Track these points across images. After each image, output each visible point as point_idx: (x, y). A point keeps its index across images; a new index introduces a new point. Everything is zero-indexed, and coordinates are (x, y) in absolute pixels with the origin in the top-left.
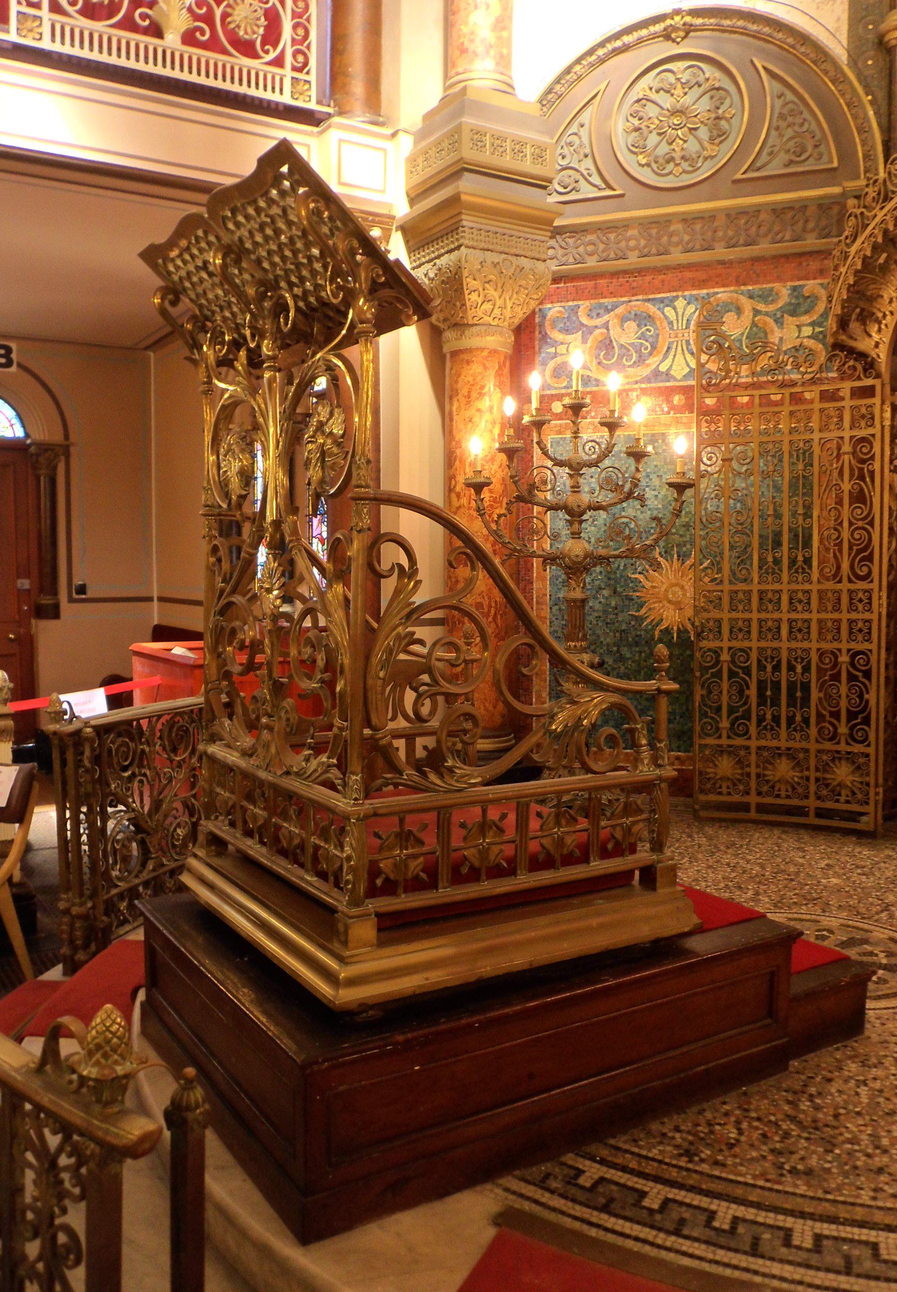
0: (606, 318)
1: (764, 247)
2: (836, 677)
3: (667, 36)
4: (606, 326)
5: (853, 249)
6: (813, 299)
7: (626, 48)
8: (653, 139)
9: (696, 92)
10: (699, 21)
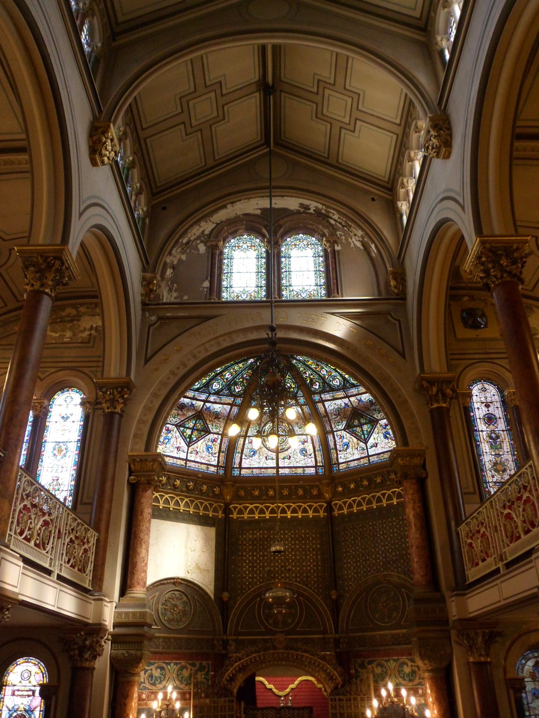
0: (152, 667)
3: (174, 583)
4: (151, 670)
5: (236, 664)
6: (205, 667)
7: (164, 584)
8: (168, 613)
9: (180, 601)
10: (182, 582)
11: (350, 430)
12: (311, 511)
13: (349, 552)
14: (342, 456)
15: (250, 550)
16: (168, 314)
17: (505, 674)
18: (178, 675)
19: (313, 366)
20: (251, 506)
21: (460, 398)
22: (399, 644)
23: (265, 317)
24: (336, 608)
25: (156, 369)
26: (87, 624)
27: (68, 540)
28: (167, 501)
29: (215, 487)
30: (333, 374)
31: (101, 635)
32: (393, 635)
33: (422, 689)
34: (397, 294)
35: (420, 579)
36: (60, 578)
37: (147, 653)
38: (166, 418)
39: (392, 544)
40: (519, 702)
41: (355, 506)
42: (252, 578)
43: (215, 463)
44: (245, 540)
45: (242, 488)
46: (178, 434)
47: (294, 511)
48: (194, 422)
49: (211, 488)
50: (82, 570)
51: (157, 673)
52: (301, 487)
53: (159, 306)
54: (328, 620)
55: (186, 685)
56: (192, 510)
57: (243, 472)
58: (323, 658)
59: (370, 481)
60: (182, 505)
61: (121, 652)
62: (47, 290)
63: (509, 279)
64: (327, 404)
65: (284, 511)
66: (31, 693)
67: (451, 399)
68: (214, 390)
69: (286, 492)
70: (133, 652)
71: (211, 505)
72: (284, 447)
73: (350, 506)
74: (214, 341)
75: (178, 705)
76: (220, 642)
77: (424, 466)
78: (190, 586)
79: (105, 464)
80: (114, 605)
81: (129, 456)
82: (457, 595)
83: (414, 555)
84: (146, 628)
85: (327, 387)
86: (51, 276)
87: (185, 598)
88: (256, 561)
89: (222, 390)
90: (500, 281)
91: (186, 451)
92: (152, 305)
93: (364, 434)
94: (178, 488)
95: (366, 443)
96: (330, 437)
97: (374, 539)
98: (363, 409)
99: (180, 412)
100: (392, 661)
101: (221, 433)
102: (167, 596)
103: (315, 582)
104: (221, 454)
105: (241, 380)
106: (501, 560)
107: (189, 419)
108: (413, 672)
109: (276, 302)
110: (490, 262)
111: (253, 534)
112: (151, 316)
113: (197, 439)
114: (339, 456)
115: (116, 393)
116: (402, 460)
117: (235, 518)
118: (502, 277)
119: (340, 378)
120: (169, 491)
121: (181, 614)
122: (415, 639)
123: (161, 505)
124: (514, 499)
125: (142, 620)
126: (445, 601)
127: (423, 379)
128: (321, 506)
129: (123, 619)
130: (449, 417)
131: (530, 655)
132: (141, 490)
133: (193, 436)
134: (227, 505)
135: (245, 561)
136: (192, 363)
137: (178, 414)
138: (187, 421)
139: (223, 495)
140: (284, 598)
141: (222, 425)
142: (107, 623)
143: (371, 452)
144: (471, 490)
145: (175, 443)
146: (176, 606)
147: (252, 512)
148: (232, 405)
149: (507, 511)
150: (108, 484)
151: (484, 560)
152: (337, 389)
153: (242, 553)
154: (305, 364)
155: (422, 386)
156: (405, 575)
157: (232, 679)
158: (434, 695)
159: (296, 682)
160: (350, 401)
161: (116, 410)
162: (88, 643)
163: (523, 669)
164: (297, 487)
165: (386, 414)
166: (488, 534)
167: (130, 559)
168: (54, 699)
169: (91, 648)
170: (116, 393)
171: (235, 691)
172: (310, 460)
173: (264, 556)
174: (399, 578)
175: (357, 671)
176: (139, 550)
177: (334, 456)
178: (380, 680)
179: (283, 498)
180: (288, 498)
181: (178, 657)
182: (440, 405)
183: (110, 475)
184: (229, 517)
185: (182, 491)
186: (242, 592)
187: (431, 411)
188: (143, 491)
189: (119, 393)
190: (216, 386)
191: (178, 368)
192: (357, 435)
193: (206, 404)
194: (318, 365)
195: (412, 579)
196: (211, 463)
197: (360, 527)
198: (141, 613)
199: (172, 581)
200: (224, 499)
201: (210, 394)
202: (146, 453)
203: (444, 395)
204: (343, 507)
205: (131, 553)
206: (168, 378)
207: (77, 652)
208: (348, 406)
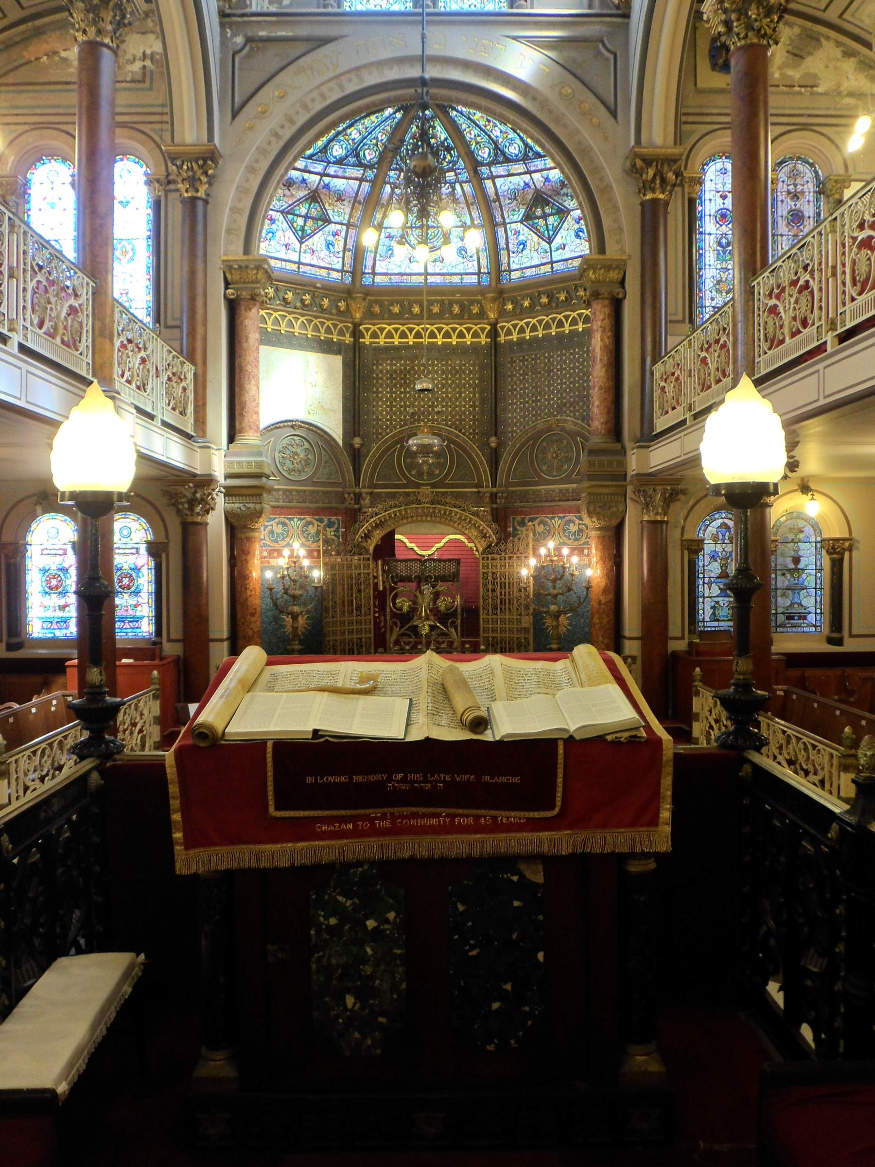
1: (321, 505)
2: (361, 646)
3: (292, 427)
6: (334, 523)
7: (280, 427)
8: (288, 462)
11: (530, 222)
12: (472, 335)
13: (516, 390)
14: (516, 260)
15: (388, 386)
16: (262, 33)
17: (682, 534)
18: (303, 532)
19: (482, 123)
20: (388, 328)
21: (686, 186)
22: (568, 500)
23: (408, 42)
24: (494, 459)
25: (251, 128)
26: (195, 475)
27: (166, 378)
28: (276, 322)
29: (340, 301)
30: (509, 137)
31: (212, 487)
32: (561, 491)
33: (588, 549)
34: (618, 7)
35: (599, 427)
36: (165, 424)
37: (267, 507)
38: (269, 203)
39: (571, 383)
40: (692, 565)
41: (528, 331)
42: (391, 420)
43: (339, 266)
44: (381, 372)
45: (376, 302)
46: (285, 225)
47: (447, 335)
48: (307, 206)
49: (334, 302)
50: (183, 413)
51: (279, 529)
52: (457, 302)
53: (246, 19)
54: (485, 472)
55: (314, 542)
56: (310, 333)
57: (378, 279)
58: (476, 514)
59: (551, 296)
60: (297, 325)
61: (236, 506)
62: (107, 41)
63: (755, 41)
64: (499, 182)
65: (432, 335)
66: (134, 551)
67: (674, 185)
68: (335, 157)
69: (436, 309)
70: (251, 505)
71: (335, 326)
72: (435, 244)
73: (522, 331)
74: (334, 82)
75: (306, 563)
76: (352, 495)
77: (622, 283)
78: (312, 430)
79: (192, 273)
80: (223, 453)
81: (223, 261)
82: (639, 447)
83: (595, 398)
84: (264, 480)
85: (500, 156)
86: (108, 16)
87: (307, 445)
88: (395, 399)
89: (347, 157)
90: (743, 42)
91: (298, 250)
92: (235, 15)
93: (548, 230)
94: (289, 303)
95: (550, 243)
96: (501, 231)
97: (549, 374)
98: (549, 193)
99: (287, 192)
100: (557, 519)
101: (345, 222)
102: (285, 442)
103: (470, 427)
104: (347, 253)
105: (374, 141)
106: (690, 410)
107: (300, 201)
108: (581, 531)
109: (429, 14)
110: (734, 11)
111: (392, 365)
112: (234, 35)
113: (313, 232)
114: (512, 259)
115: (195, 167)
116: (594, 273)
117: (367, 343)
118: (746, 37)
119: (521, 144)
120: (279, 308)
121: (303, 462)
122: (584, 495)
123: (270, 327)
124: (712, 341)
125: (259, 471)
126: (625, 452)
127: (636, 155)
128: (483, 330)
129: (236, 470)
130: (666, 213)
131: (717, 516)
132: (243, 308)
133: (306, 228)
134: (356, 326)
135: (381, 399)
136: (302, 119)
137: (284, 196)
138: (298, 205)
139: (350, 312)
140: (430, 446)
141: (348, 210)
142: (216, 474)
143: (557, 256)
144: (680, 317)
145: (282, 238)
146: (296, 454)
147: (389, 335)
148: (361, 180)
149: (704, 354)
150: (199, 302)
151: (674, 408)
152: (515, 161)
153: (377, 389)
154: (469, 119)
155: (634, 165)
156: (583, 421)
157: (367, 536)
158: (599, 554)
159: (444, 541)
160: (532, 178)
161: (199, 195)
162: (198, 495)
163: (705, 531)
164: (451, 303)
165: (580, 204)
166: (681, 378)
167: (237, 398)
168: (164, 556)
169: (203, 501)
170: (195, 167)
171: (371, 549)
172: (470, 264)
173: (405, 392)
174: (576, 424)
175: (515, 529)
176: (247, 386)
177: (504, 259)
178: (539, 539)
179: (432, 317)
180: (440, 316)
181: (302, 512)
182: (655, 196)
183: (199, 289)
184: (359, 342)
185: (295, 308)
186: (377, 437)
187: (642, 204)
188: (246, 310)
189: (200, 167)
190: (338, 151)
191: (282, 127)
192: (538, 230)
193: (324, 178)
194: (489, 121)
195: (589, 426)
196: (334, 267)
197: (533, 359)
198: (257, 463)
199: (290, 424)
200: (352, 317)
201: (329, 162)
202: (244, 257)
203: (664, 181)
204: (513, 331)
205: (237, 389)
206: (269, 143)
207: (186, 506)
208: (529, 187)
